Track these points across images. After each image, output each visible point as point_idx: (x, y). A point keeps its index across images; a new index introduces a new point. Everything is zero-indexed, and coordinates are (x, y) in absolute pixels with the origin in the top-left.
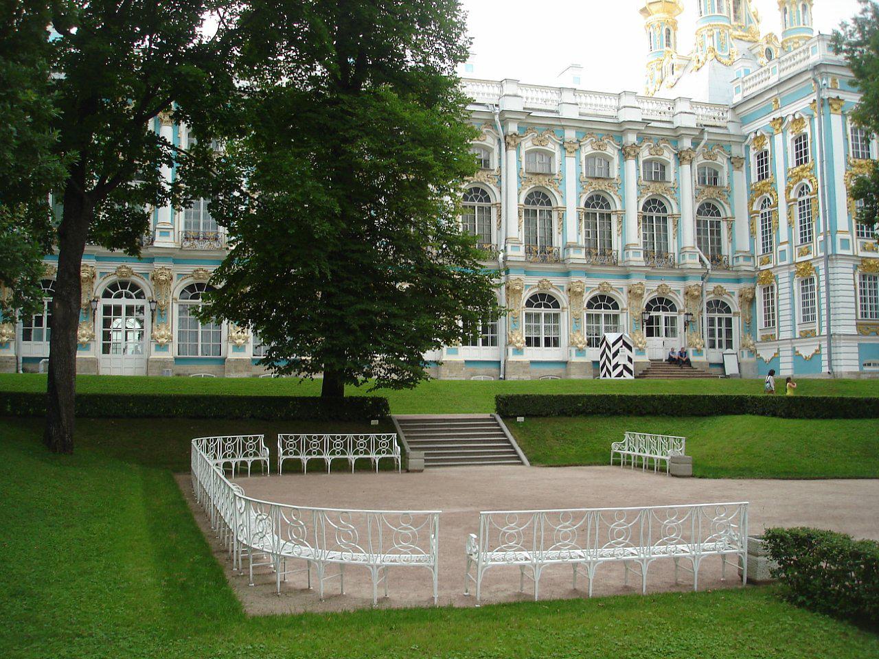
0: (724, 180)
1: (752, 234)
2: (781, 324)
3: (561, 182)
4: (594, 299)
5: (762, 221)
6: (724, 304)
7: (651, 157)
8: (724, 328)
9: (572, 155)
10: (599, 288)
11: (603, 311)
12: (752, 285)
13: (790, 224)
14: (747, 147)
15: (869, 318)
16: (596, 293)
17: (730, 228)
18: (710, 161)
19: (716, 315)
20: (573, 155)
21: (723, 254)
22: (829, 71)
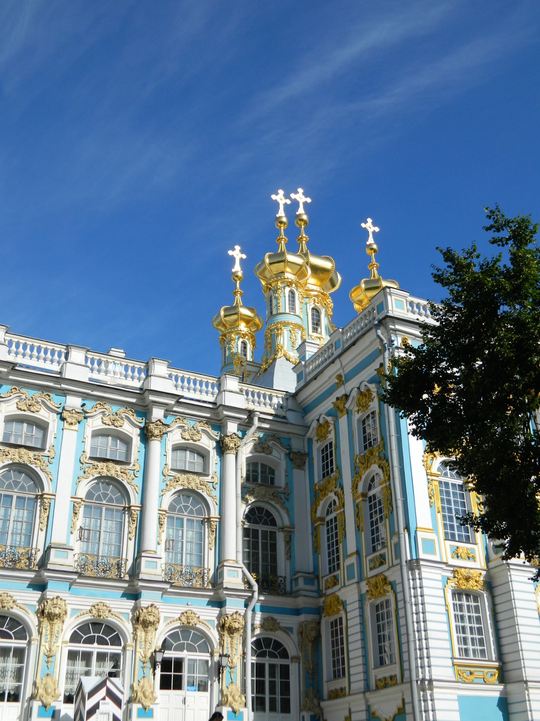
0: (281, 480)
1: (316, 549)
2: (352, 672)
3: (52, 460)
4: (84, 628)
5: (328, 530)
6: (278, 645)
7: (184, 441)
8: (278, 680)
9: (73, 427)
10: (90, 611)
11: (95, 648)
12: (316, 617)
13: (358, 528)
14: (310, 440)
15: (472, 657)
16: (88, 617)
17: (289, 542)
18: (263, 454)
19: (267, 661)
20: (76, 427)
21: (279, 574)
22: (398, 327)
